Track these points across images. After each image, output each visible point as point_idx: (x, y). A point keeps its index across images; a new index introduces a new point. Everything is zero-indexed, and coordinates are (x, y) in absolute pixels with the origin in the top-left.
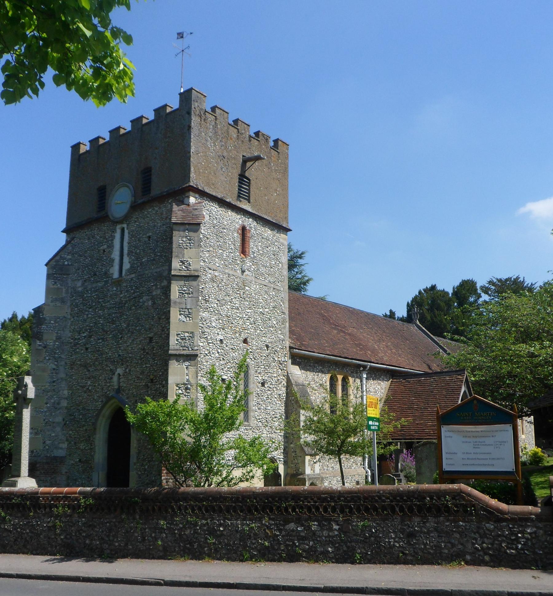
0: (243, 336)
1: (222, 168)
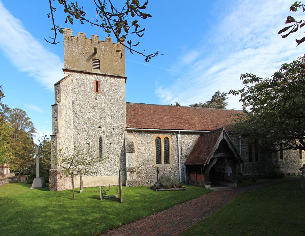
0: (98, 125)
1: (82, 59)
